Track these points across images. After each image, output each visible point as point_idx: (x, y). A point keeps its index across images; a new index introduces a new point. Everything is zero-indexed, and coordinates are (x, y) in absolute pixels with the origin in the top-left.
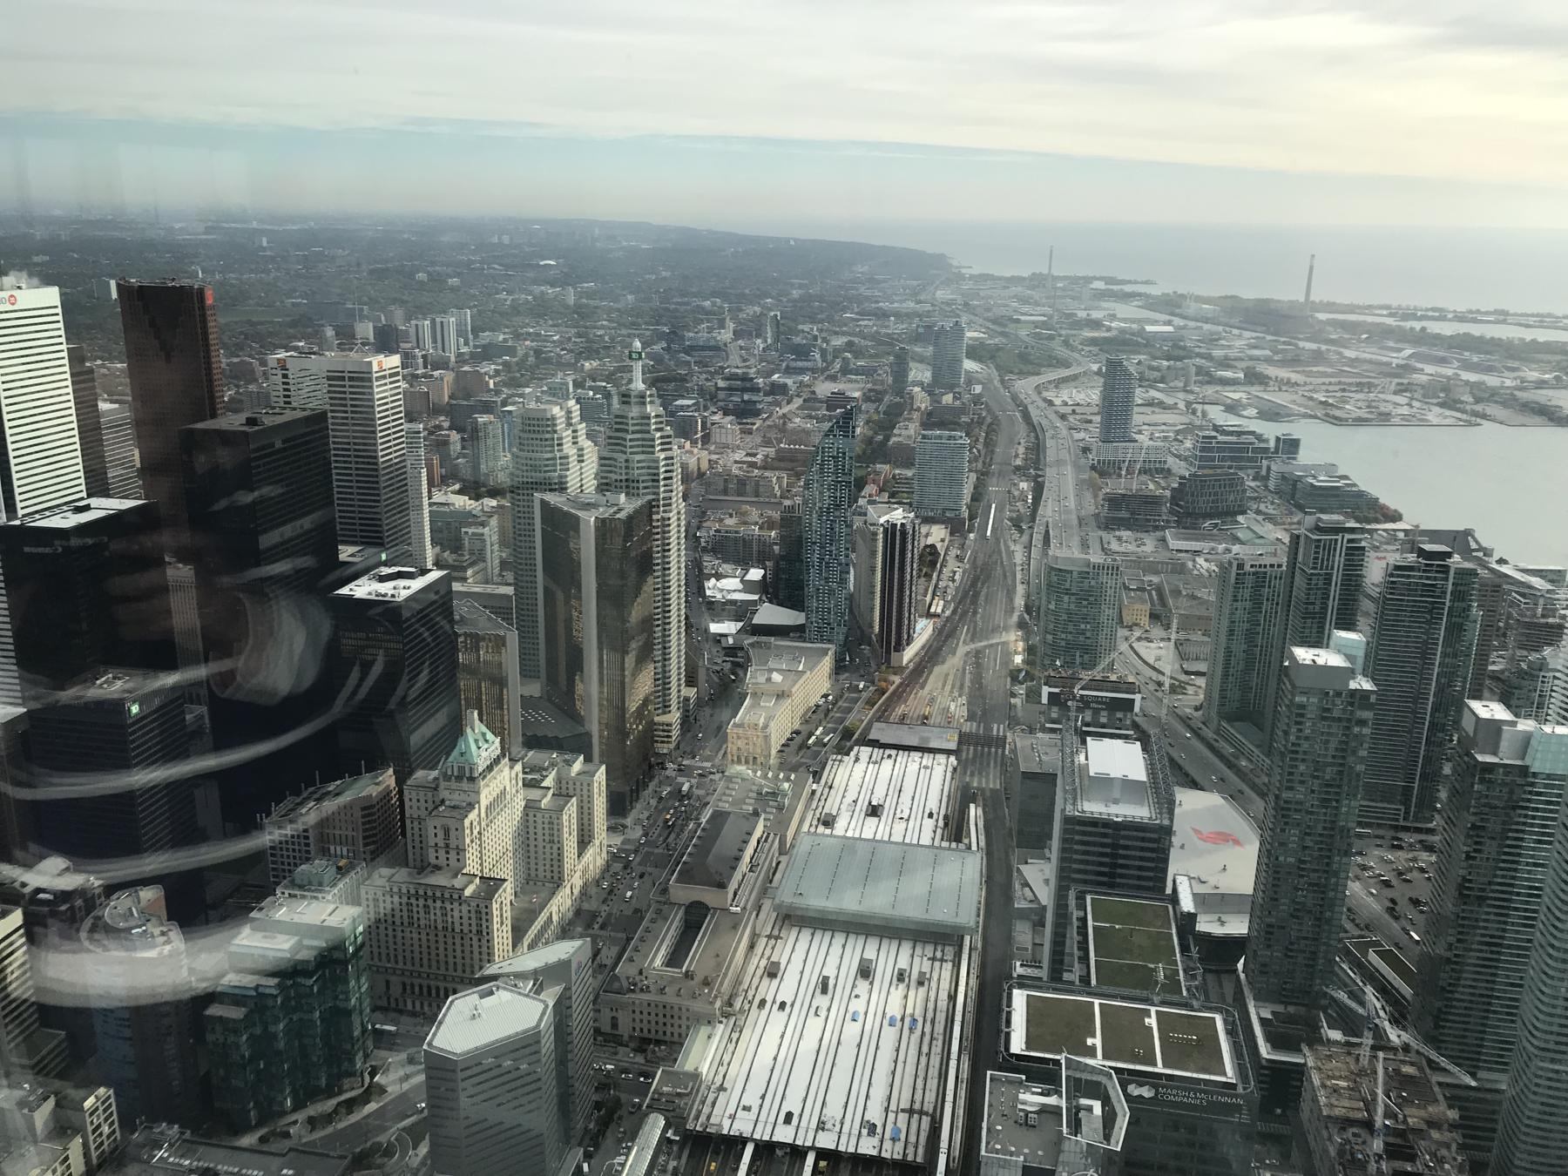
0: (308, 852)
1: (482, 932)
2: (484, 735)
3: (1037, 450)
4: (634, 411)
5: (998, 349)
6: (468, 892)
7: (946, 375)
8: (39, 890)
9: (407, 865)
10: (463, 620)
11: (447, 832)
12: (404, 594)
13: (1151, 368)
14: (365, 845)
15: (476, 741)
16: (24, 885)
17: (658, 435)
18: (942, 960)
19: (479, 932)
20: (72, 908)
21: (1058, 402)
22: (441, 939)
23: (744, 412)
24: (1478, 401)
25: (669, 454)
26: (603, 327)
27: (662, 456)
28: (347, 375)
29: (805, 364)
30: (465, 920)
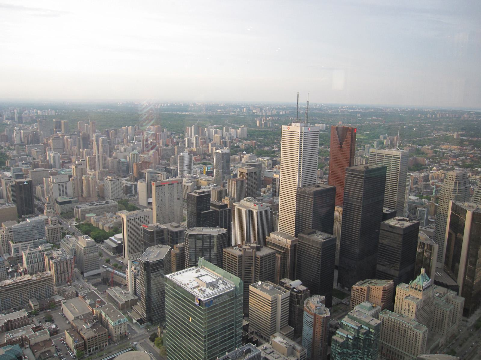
0: (364, 299)
2: (426, 277)
9: (393, 311)
14: (382, 302)
15: (423, 278)
16: (291, 285)
19: (416, 341)
22: (402, 339)
28: (392, 156)
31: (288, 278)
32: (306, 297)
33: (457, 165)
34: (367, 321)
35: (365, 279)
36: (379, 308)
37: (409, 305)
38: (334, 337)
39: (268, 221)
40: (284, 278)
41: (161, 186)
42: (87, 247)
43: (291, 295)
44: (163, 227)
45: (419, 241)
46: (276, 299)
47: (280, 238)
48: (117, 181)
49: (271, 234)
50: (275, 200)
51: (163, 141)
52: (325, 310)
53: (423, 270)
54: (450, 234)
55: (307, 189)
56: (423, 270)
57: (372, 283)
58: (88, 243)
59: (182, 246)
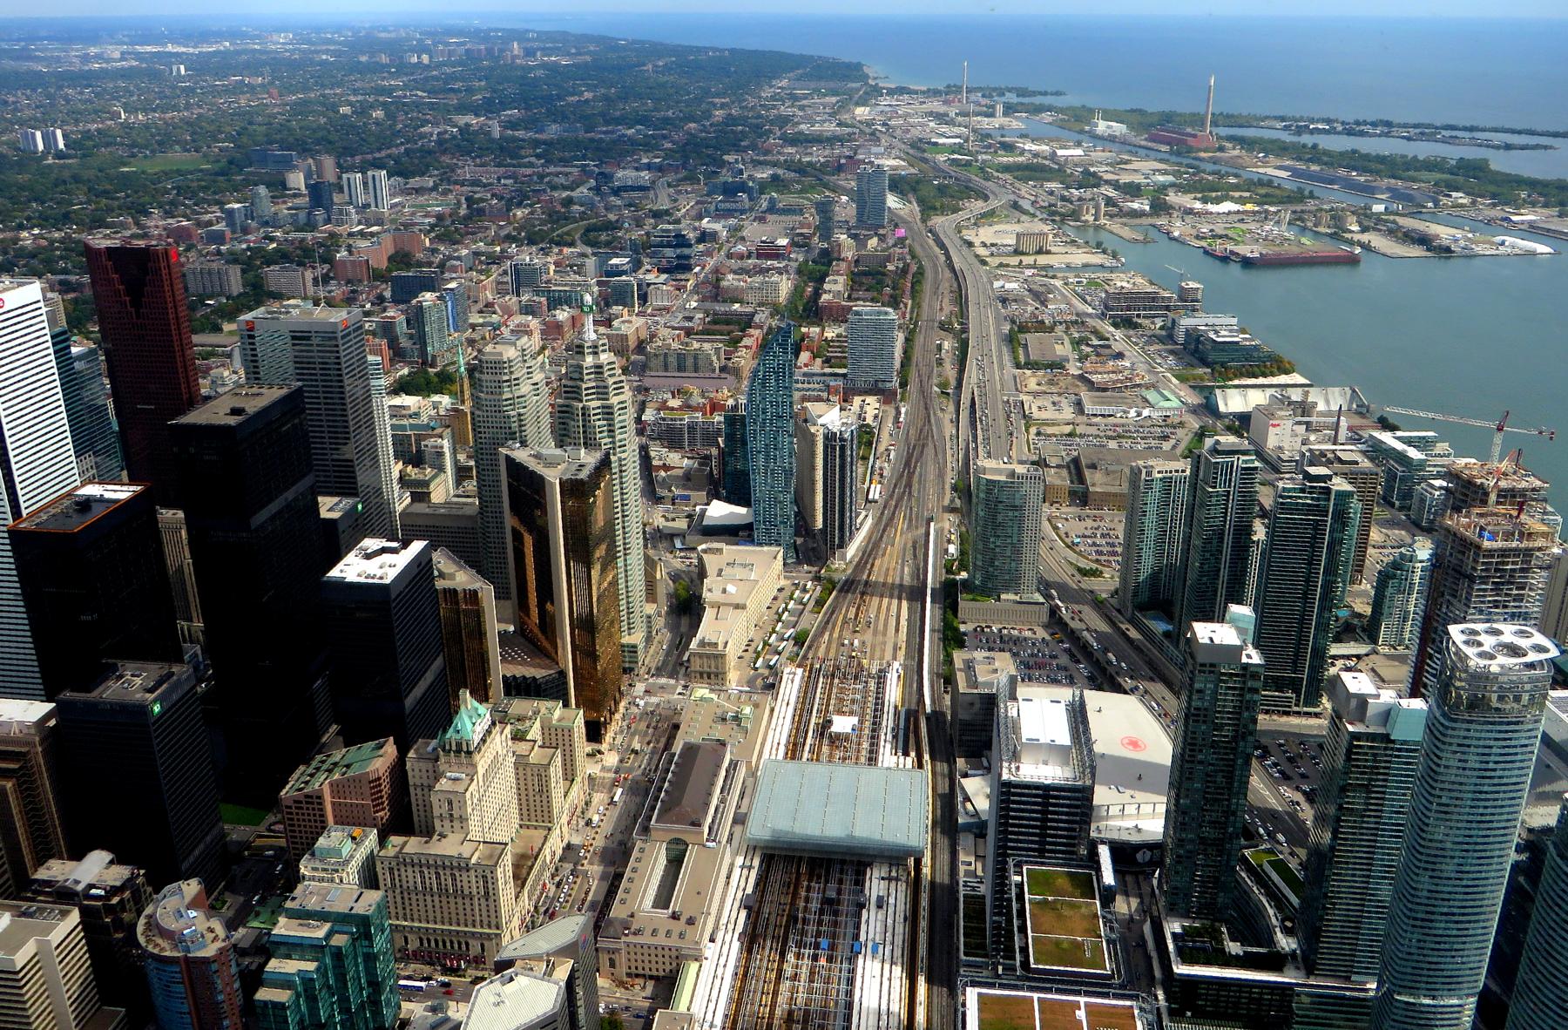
1: (489, 894)
3: (960, 299)
4: (589, 360)
5: (918, 182)
6: (473, 861)
7: (870, 217)
8: (92, 886)
10: (442, 575)
11: (450, 803)
12: (390, 576)
13: (1063, 199)
16: (77, 882)
17: (611, 381)
18: (897, 879)
19: (487, 893)
20: (122, 900)
21: (977, 242)
23: (679, 267)
24: (1364, 230)
25: (621, 398)
26: (531, 165)
27: (611, 381)
29: (734, 206)
32: (139, 903)
33: (510, 239)
34: (341, 907)
35: (313, 758)
36: (373, 835)
37: (450, 803)
38: (263, 994)
43: (85, 912)
45: (440, 584)
52: (211, 930)
53: (466, 695)
54: (517, 537)
56: (466, 695)
57: (335, 764)
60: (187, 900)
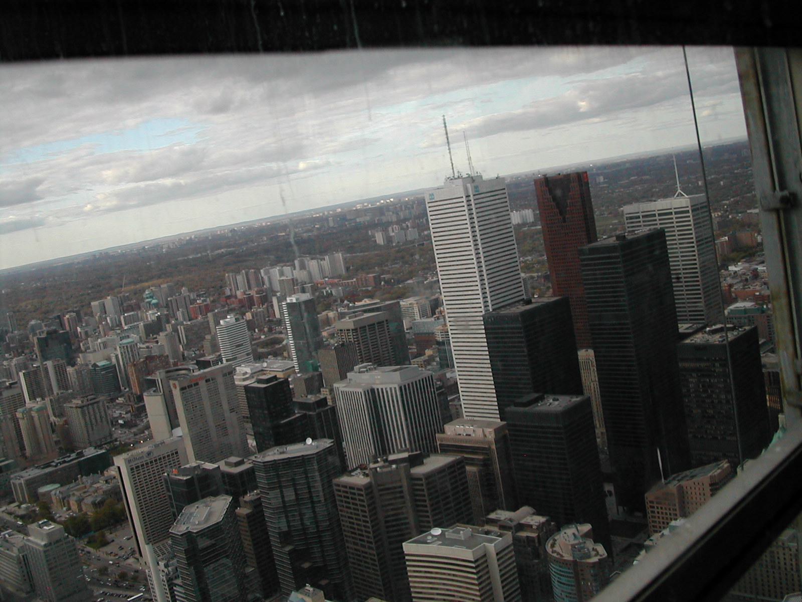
16: (511, 520)
30: (788, 561)
31: (502, 509)
39: (435, 402)
40: (493, 510)
41: (191, 386)
42: (50, 544)
43: (516, 540)
44: (209, 466)
45: (764, 370)
46: (485, 555)
47: (469, 429)
48: (95, 405)
49: (447, 427)
50: (448, 375)
51: (183, 313)
55: (504, 312)
58: (50, 534)
59: (256, 497)
60: (581, 533)
